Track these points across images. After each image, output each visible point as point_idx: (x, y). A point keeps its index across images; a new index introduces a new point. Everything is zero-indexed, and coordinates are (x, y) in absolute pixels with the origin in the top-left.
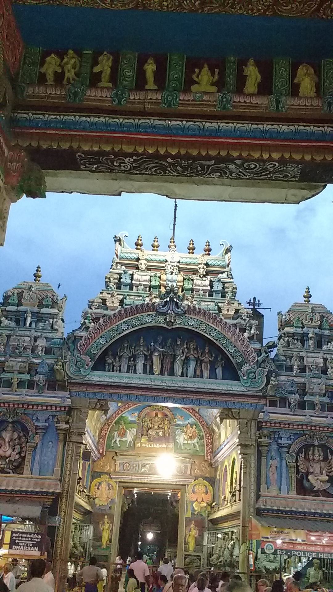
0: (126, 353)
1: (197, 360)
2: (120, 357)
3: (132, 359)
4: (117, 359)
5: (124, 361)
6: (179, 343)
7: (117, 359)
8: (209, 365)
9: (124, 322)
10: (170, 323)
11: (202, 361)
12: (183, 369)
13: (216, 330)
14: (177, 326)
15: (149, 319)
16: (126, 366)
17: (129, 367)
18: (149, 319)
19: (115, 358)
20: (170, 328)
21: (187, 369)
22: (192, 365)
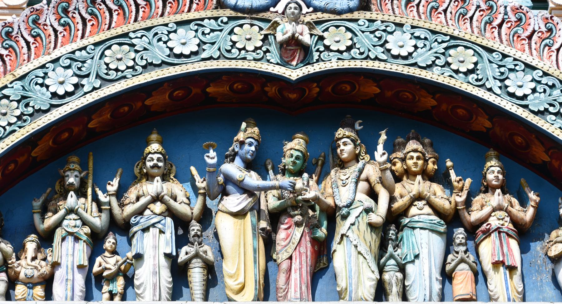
0: (79, 211)
1: (452, 219)
2: (46, 240)
3: (109, 243)
4: (31, 246)
5: (70, 254)
6: (346, 149)
7: (31, 246)
8: (514, 244)
9: (55, 61)
10: (293, 48)
11: (473, 231)
12: (381, 270)
13: (530, 67)
14: (332, 63)
15: (185, 41)
16: (80, 280)
17: (94, 281)
18: (185, 41)
19: (20, 249)
20: (294, 73)
21: (402, 269)
22: (423, 244)
